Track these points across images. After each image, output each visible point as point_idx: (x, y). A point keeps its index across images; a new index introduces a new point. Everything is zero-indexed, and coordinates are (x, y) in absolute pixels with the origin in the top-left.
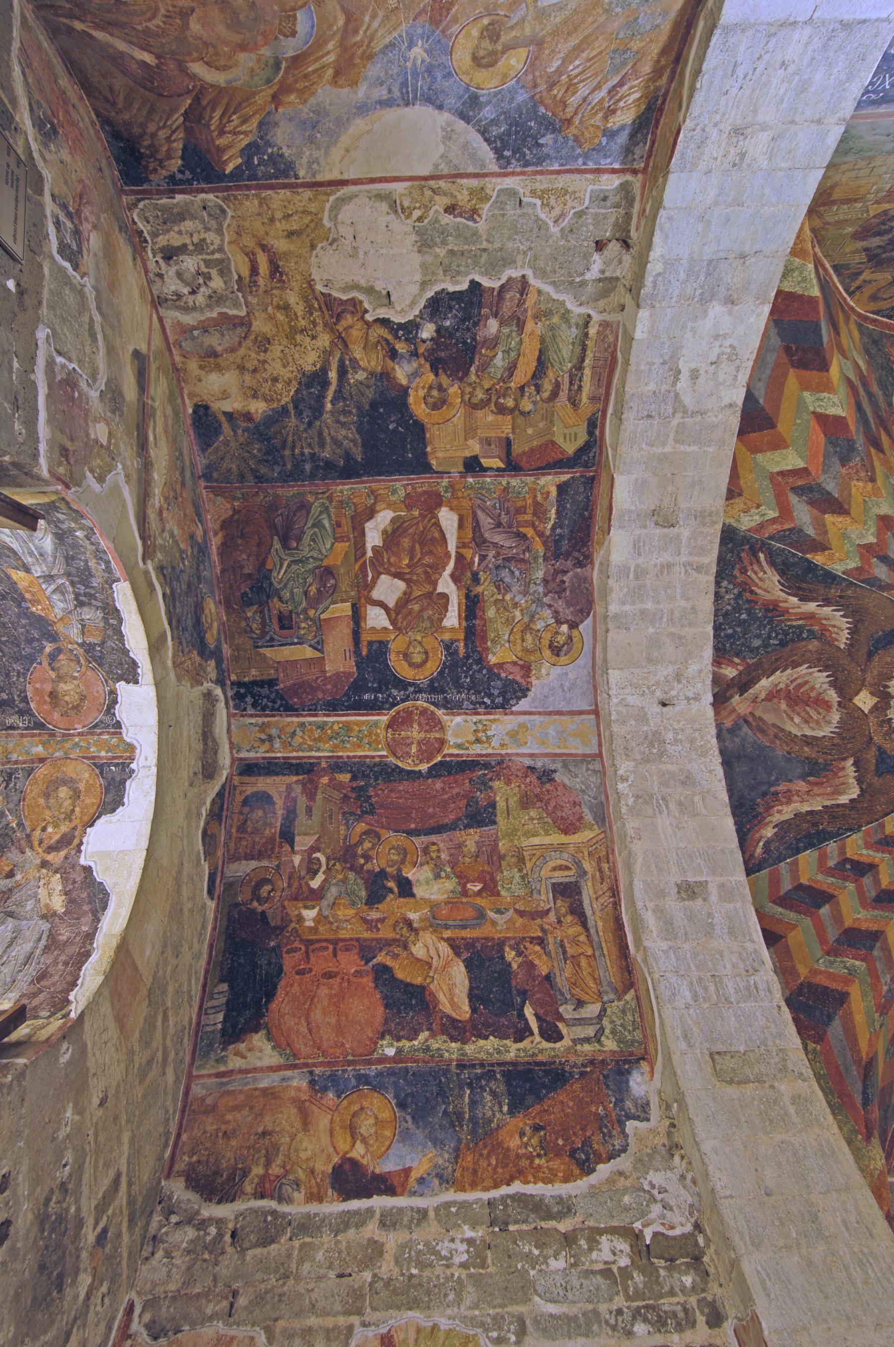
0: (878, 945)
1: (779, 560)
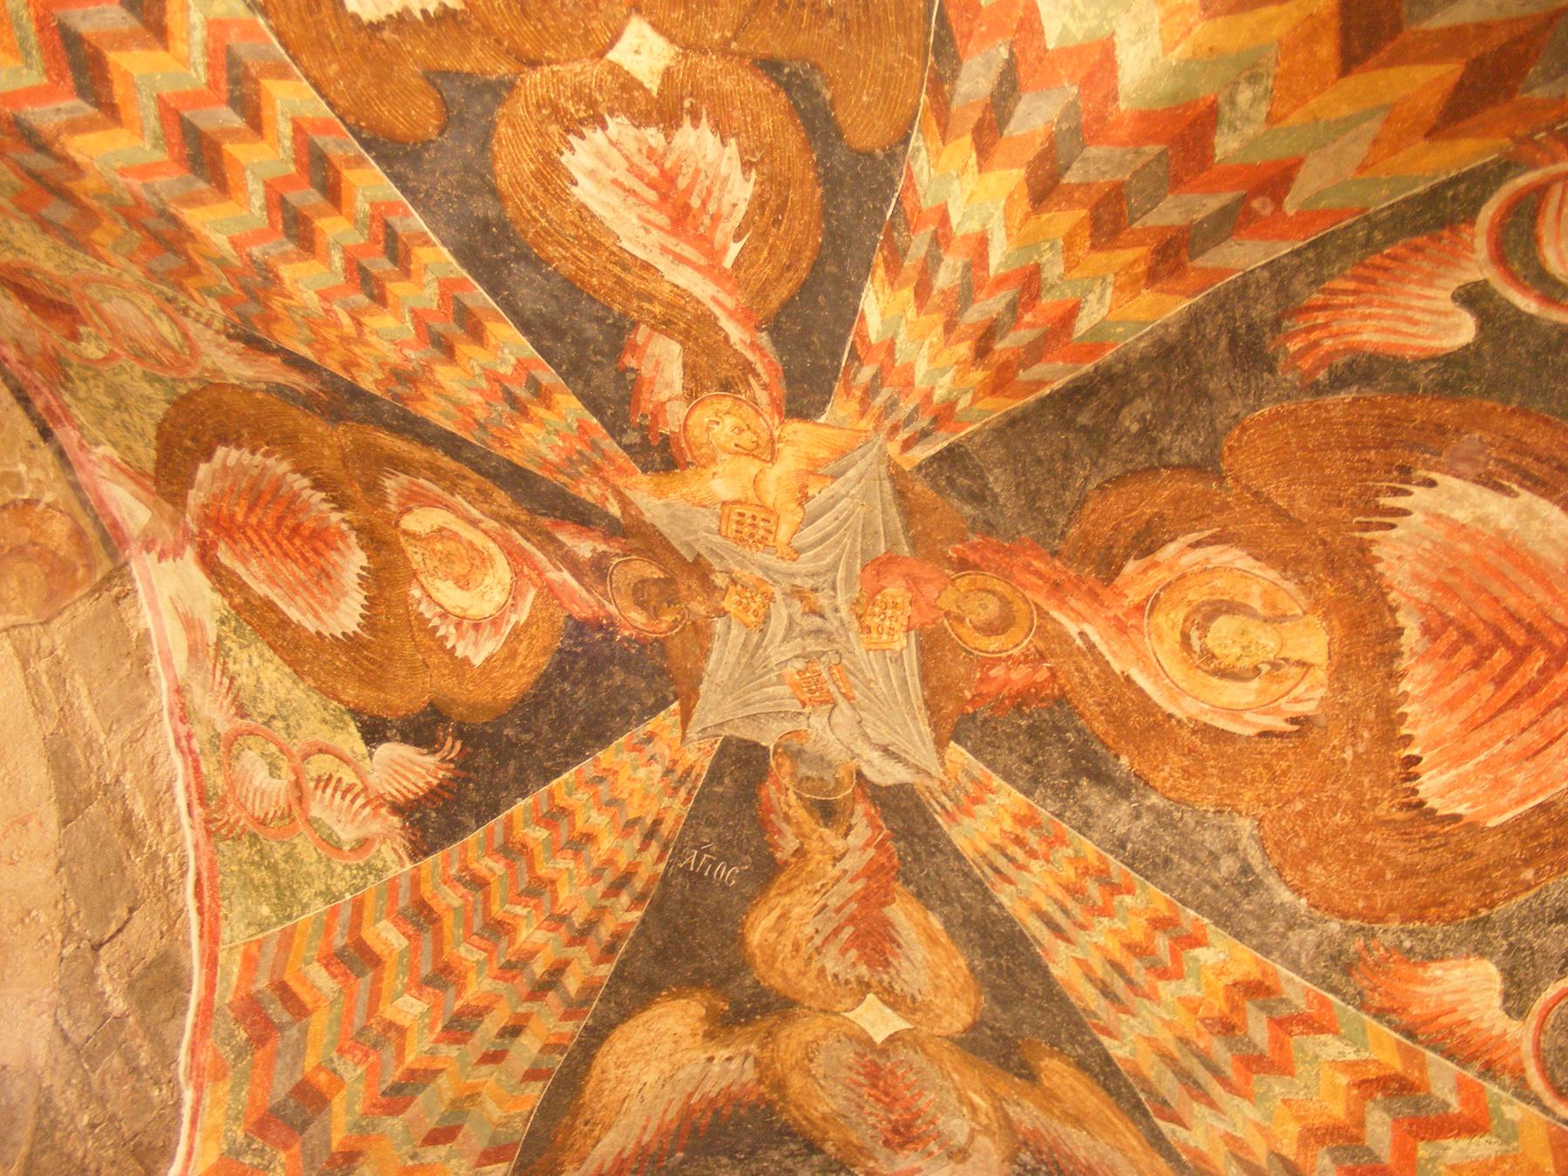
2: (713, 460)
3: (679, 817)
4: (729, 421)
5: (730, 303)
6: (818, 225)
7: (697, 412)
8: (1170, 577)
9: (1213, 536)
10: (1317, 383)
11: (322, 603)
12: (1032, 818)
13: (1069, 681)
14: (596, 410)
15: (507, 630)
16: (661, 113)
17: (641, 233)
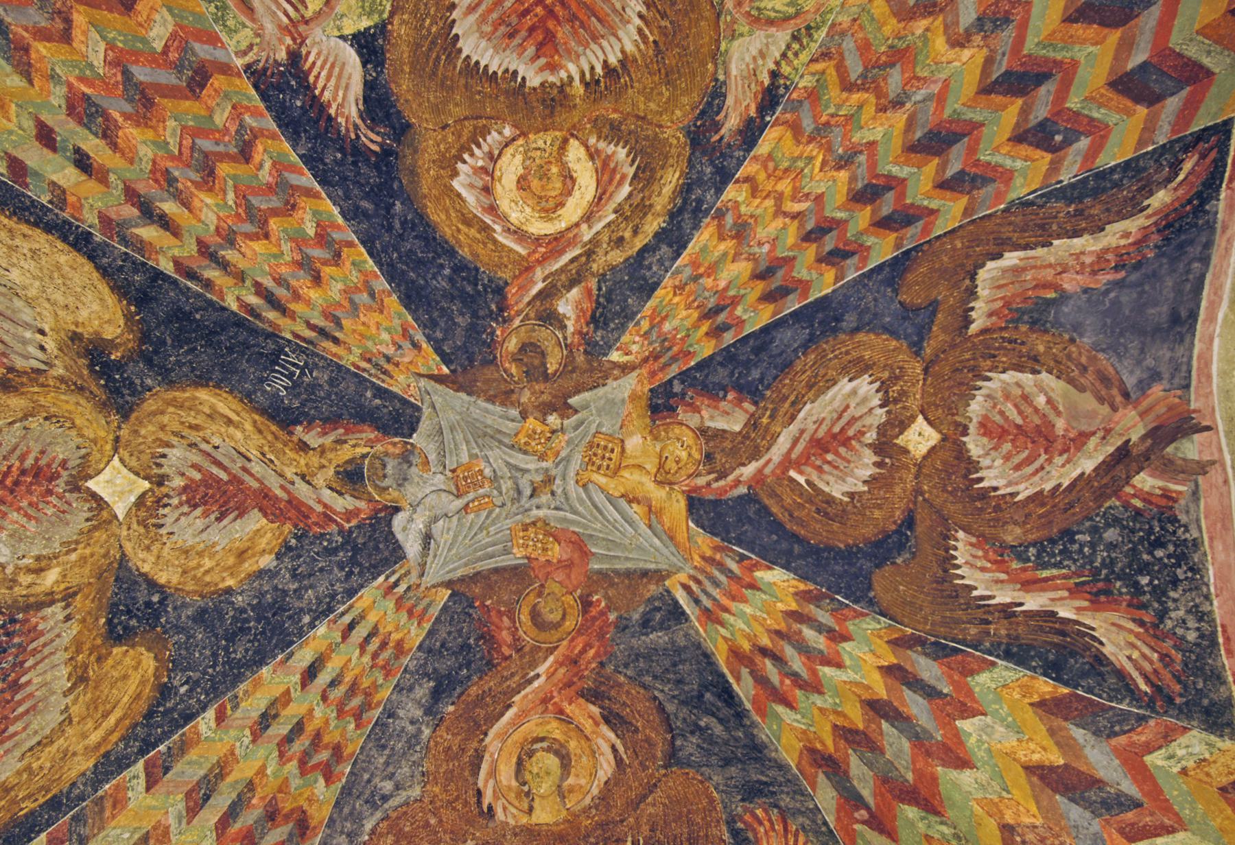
2: (656, 438)
3: (340, 358)
4: (684, 455)
5: (767, 471)
6: (821, 542)
7: (690, 433)
8: (588, 731)
9: (622, 759)
10: (735, 822)
12: (402, 653)
13: (504, 668)
14: (700, 366)
15: (488, 220)
16: (884, 443)
17: (814, 418)
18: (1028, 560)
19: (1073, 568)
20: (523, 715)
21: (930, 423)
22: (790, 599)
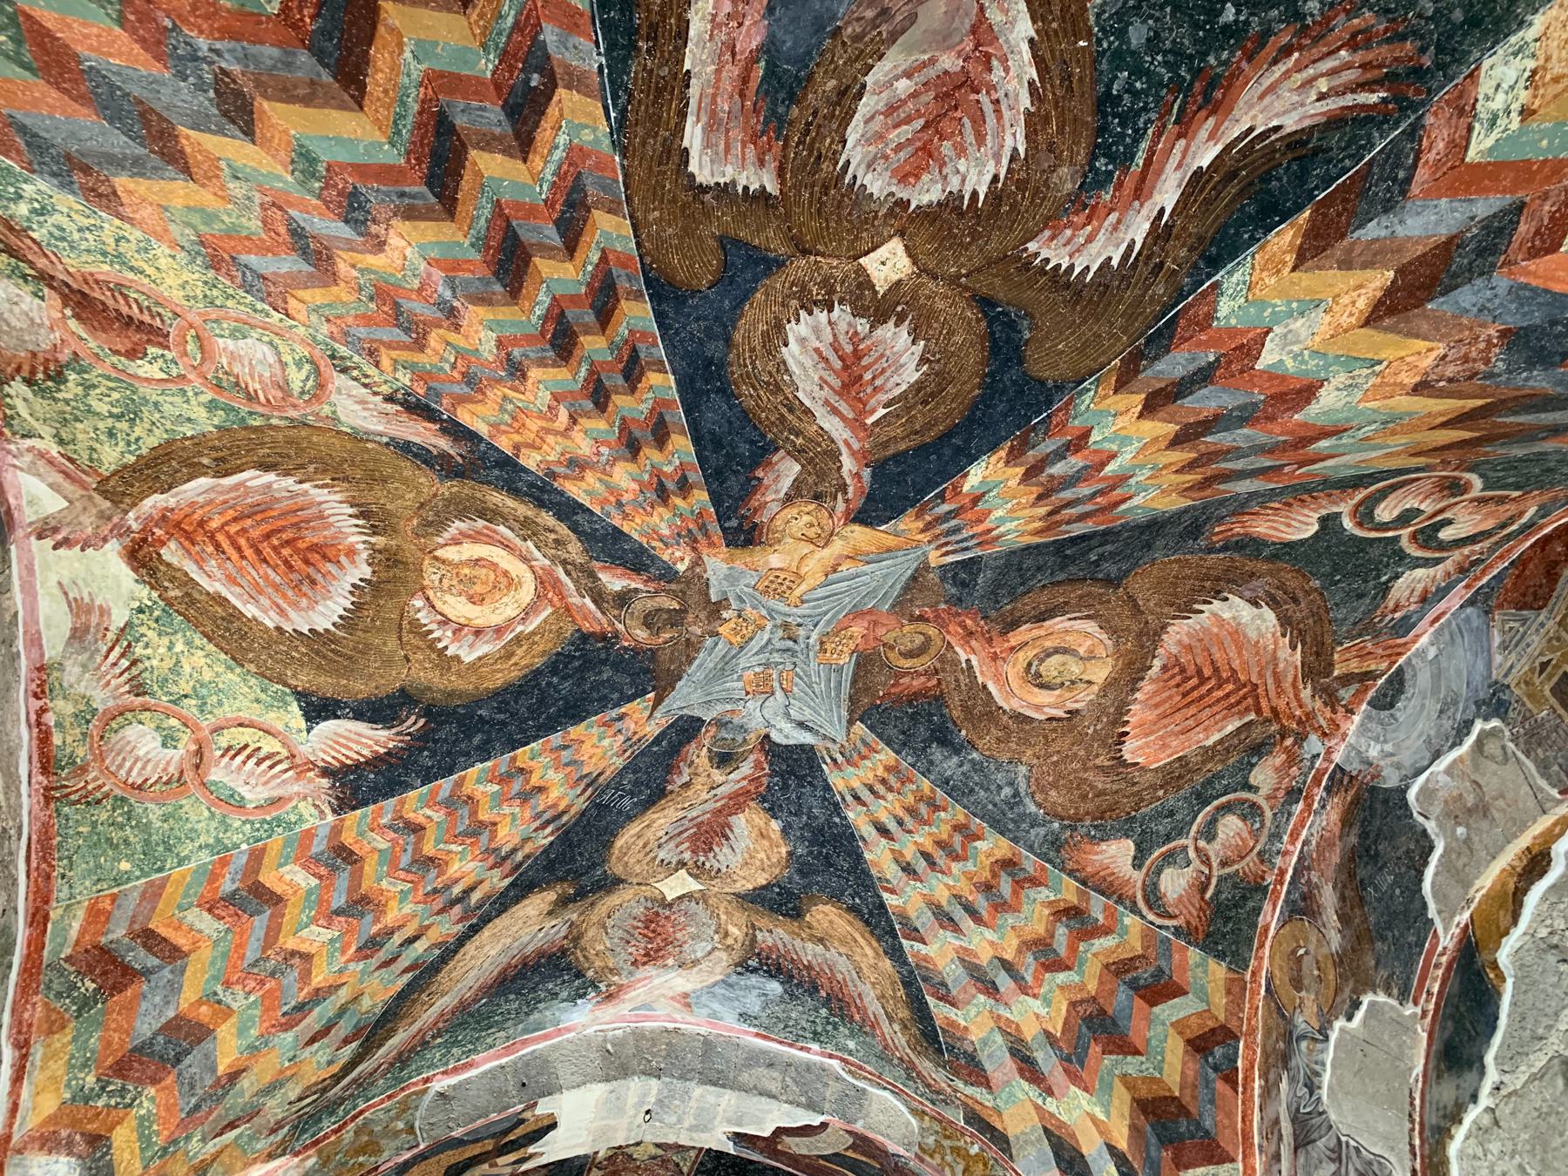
0: (326, 77)
1: (1334, 139)
4: (806, 518)
11: (295, 605)
16: (877, 310)
18: (1111, 173)
19: (1154, 116)
20: (1003, 681)
21: (873, 249)
22: (1011, 471)
